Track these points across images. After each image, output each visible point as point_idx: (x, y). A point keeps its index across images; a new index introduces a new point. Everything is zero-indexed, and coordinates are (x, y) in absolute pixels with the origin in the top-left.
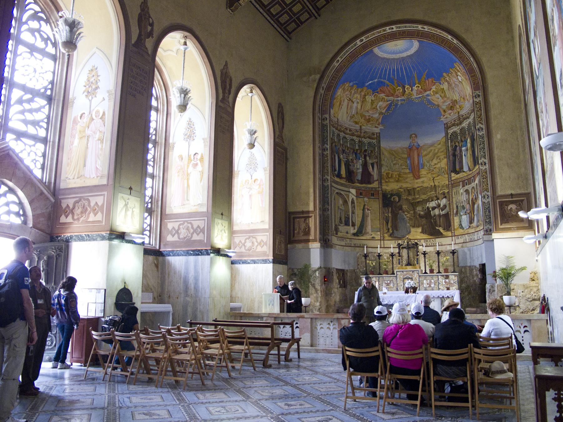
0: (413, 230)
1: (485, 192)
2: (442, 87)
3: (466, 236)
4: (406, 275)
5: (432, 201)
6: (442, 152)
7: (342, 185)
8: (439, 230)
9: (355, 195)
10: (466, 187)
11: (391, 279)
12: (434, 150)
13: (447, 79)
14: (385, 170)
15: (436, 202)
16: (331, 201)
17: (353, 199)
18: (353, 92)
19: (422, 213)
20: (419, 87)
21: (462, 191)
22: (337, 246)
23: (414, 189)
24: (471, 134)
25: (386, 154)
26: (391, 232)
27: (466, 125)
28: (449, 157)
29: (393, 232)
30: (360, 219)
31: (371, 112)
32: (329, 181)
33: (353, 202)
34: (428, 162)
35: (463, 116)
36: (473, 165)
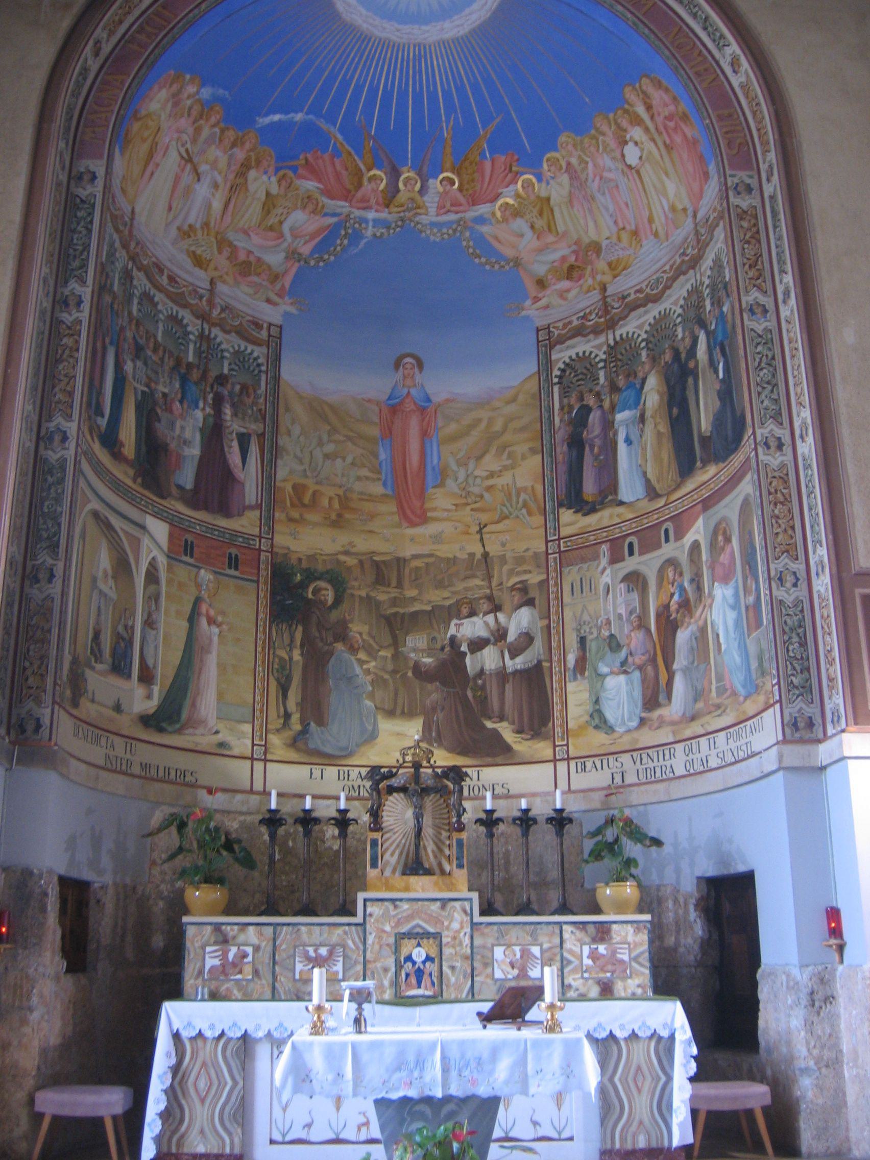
0: (386, 726)
1: (785, 560)
2: (541, 189)
3: (625, 758)
4: (410, 917)
5: (472, 614)
6: (522, 429)
7: (116, 486)
8: (496, 734)
9: (165, 548)
10: (631, 564)
11: (334, 939)
12: (491, 421)
13: (574, 161)
14: (291, 472)
15: (490, 618)
16: (70, 537)
17: (153, 564)
18: (206, 132)
19: (428, 660)
20: (452, 183)
21: (606, 578)
22: (73, 762)
23: (400, 562)
24: (668, 357)
25: (299, 409)
26: (298, 727)
27: (640, 327)
28: (553, 447)
29: (305, 731)
30: (176, 657)
31: (256, 239)
32: (72, 445)
33: (152, 577)
34: (462, 463)
35: (624, 298)
36: (672, 474)
